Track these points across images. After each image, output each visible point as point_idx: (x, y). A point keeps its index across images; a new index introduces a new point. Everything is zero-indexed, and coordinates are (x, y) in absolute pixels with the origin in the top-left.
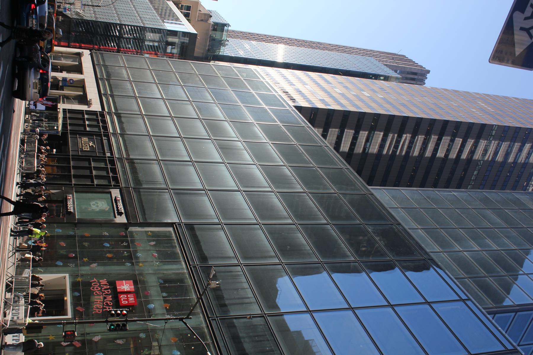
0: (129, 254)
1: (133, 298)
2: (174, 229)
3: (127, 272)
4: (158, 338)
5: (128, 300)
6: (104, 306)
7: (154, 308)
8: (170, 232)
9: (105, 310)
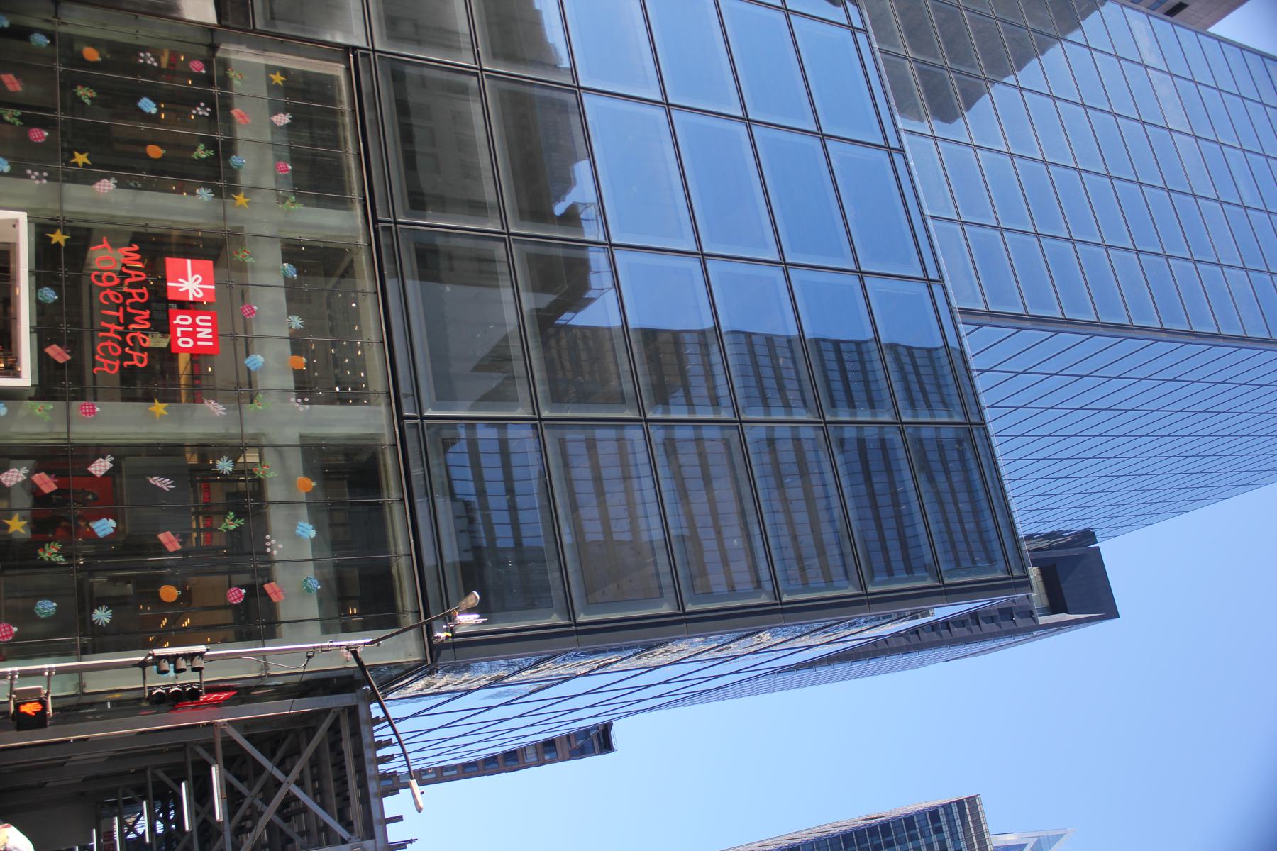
0: (211, 153)
1: (210, 330)
2: (348, 69)
3: (201, 220)
4: (263, 477)
5: (193, 335)
6: (127, 349)
7: (263, 369)
8: (333, 79)
9: (130, 363)
